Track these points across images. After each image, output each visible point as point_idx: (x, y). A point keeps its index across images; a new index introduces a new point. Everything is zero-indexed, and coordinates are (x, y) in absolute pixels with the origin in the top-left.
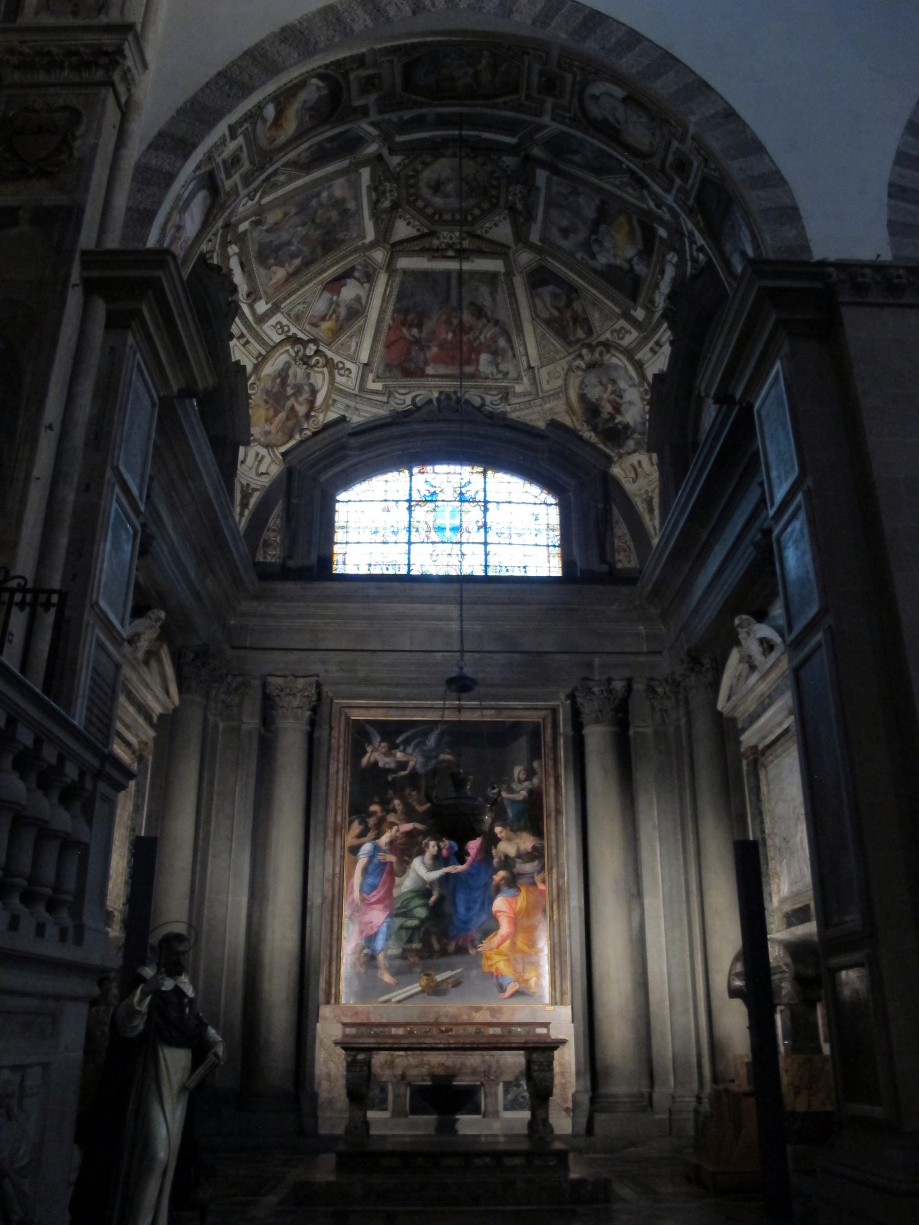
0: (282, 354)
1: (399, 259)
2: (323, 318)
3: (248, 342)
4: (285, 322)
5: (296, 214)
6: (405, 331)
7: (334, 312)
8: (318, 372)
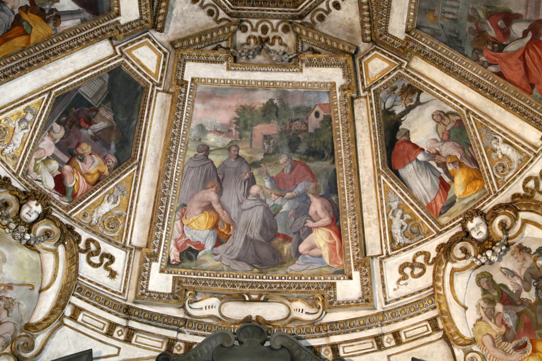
0: (452, 283)
1: (390, 32)
2: (445, 187)
4: (407, 256)
5: (220, 192)
6: (511, 48)
7: (443, 165)
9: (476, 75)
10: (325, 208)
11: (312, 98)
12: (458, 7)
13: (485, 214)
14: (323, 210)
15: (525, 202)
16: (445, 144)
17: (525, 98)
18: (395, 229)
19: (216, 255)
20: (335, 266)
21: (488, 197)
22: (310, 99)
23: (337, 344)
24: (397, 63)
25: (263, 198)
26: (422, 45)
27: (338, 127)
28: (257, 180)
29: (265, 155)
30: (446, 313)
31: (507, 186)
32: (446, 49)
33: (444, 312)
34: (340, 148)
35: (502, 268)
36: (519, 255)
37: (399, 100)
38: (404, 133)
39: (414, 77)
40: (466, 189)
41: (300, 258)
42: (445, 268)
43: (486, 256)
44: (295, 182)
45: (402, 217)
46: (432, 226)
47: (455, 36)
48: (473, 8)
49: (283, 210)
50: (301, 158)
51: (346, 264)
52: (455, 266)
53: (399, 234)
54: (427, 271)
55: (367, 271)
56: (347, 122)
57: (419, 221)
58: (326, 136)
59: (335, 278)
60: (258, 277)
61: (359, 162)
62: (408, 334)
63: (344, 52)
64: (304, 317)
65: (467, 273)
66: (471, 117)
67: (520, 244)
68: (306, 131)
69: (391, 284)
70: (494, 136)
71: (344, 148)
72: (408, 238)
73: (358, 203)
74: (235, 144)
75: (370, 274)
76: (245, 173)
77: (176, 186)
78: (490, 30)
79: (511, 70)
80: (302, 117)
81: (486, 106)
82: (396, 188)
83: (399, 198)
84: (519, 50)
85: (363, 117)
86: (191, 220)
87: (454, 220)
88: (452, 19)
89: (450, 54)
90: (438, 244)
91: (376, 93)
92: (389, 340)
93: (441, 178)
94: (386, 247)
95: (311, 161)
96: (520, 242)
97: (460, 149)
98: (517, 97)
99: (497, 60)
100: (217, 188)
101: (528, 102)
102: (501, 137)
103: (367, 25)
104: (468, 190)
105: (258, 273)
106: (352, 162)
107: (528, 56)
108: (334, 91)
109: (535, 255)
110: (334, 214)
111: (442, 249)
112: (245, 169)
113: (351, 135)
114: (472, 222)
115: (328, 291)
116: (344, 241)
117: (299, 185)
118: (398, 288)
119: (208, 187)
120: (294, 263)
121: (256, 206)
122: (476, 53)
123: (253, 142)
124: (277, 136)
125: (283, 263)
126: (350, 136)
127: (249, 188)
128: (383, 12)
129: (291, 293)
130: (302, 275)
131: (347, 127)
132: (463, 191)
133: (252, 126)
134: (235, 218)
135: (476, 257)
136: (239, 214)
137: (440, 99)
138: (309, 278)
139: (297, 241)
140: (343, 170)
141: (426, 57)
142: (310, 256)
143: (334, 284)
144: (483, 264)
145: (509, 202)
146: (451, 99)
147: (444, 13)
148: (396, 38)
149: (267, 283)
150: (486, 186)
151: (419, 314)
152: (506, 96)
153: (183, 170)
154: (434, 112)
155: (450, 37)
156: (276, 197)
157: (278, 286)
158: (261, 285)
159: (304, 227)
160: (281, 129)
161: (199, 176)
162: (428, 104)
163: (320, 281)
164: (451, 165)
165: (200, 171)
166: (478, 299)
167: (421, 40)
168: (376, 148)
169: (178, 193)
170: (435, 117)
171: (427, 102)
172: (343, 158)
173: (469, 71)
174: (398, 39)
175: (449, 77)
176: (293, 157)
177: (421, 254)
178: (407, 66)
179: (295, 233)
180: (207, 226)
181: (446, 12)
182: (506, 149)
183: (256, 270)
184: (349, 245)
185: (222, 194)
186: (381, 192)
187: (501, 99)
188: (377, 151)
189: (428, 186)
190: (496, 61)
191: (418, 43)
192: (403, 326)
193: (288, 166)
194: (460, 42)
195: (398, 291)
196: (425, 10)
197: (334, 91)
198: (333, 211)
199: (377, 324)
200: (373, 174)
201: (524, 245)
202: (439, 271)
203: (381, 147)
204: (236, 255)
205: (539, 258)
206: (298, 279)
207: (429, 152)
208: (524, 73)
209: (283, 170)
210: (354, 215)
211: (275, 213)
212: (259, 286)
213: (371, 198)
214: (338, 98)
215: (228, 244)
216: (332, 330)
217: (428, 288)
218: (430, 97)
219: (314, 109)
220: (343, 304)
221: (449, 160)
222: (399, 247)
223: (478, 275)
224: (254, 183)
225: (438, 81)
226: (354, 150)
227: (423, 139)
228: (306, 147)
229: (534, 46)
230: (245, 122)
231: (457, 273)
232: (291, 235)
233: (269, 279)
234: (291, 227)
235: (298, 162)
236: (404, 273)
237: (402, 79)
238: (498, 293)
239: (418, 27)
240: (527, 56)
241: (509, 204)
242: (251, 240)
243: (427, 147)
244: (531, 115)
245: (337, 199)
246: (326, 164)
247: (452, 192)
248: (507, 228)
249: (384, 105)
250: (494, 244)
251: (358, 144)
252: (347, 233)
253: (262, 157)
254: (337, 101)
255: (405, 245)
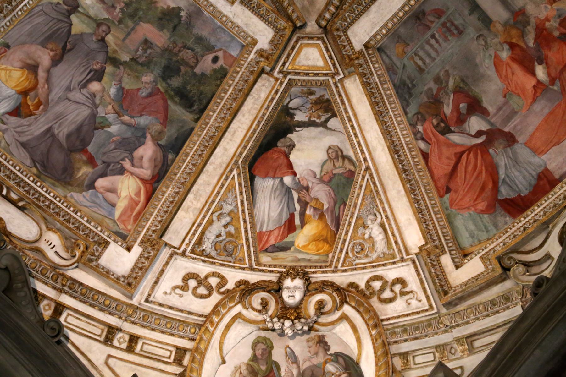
0: (228, 327)
1: (349, 33)
3: (133, 339)
4: (203, 269)
5: (56, 61)
6: (455, 138)
7: (304, 205)
8: (333, 323)
9: (402, 139)
10: (154, 160)
11: (223, 40)
12: (434, 59)
13: (310, 283)
14: (150, 160)
15: (358, 298)
16: (321, 185)
17: (432, 197)
18: (210, 232)
19: (3, 123)
20: (122, 226)
21: (326, 267)
22: (220, 39)
23: (65, 307)
24: (332, 69)
25: (98, 102)
26: (371, 71)
27: (228, 88)
28: (105, 78)
29: (132, 59)
30: (202, 353)
31: (353, 270)
32: (392, 92)
33: (200, 351)
34: (214, 111)
35: (288, 347)
36: (314, 346)
37: (307, 107)
38: (288, 144)
39: (340, 95)
40: (309, 244)
41: (90, 191)
42: (232, 307)
43: (283, 324)
44: (143, 110)
45: (225, 226)
46: (249, 256)
47: (410, 85)
48: (447, 71)
49: (108, 129)
50: (166, 91)
51: (134, 232)
52: (245, 312)
53: (211, 241)
54: (211, 297)
55: (152, 254)
56: (241, 90)
57: (240, 242)
58: (208, 88)
59: (112, 238)
60: (31, 179)
61: (223, 140)
62: (146, 347)
63: (289, 18)
64: (51, 254)
65: (251, 328)
66: (367, 176)
67: (323, 336)
68: (192, 68)
69: (166, 284)
70: (376, 212)
71: (218, 114)
72: (217, 251)
73: (193, 179)
74: (109, 24)
75: (152, 260)
76: (98, 63)
77: (14, 19)
78: (448, 105)
79: (440, 159)
80: (199, 50)
81: (388, 177)
82: (241, 193)
83: (237, 205)
84: (462, 145)
85: (259, 97)
86: (4, 66)
87: (275, 266)
88: (419, 67)
89: (392, 99)
90: (243, 278)
91: (291, 83)
92: (122, 340)
93: (292, 216)
94: (188, 244)
95: (175, 103)
96: (324, 334)
97: (332, 201)
98: (426, 190)
99: (433, 139)
100: (56, 55)
101: (433, 202)
102: (382, 218)
103: (332, 9)
104: (310, 247)
105: (35, 175)
106: (216, 134)
107: (466, 159)
108: (251, 49)
109: (330, 357)
110: (158, 173)
111: (243, 287)
112: (101, 57)
113: (236, 106)
114: (293, 279)
115: (96, 246)
116: (150, 208)
117: (145, 117)
118: (170, 294)
119: (48, 46)
120: (81, 192)
121: (84, 104)
122: (418, 117)
123: (129, 37)
124: (159, 50)
125: (69, 184)
126: (233, 106)
127: (90, 81)
128: (357, 8)
129: (55, 220)
130: (80, 211)
131: (237, 95)
132: (305, 244)
133: (140, 19)
134: (52, 101)
135: (271, 317)
136: (60, 100)
137: (349, 137)
138: (86, 219)
139: (100, 172)
140: (201, 135)
141: (366, 85)
142: (103, 197)
143: (107, 244)
144: (273, 330)
145: (342, 286)
146: (360, 145)
147: (416, 54)
148: (351, 43)
149: (37, 191)
150: (331, 255)
151: (172, 335)
152: (416, 181)
153: (33, 8)
154: (333, 146)
155: (404, 84)
156: (112, 111)
157: (47, 203)
158: (30, 189)
159: (118, 163)
160: (168, 46)
161: (46, 28)
162: (333, 132)
163: (95, 230)
164: (312, 210)
165: (51, 24)
166: (242, 361)
167: (373, 64)
168: (250, 138)
169: (10, 29)
170: (330, 151)
171: (334, 130)
172: (210, 123)
173: (398, 131)
174: (352, 46)
175: (375, 121)
176: (159, 83)
177: (218, 277)
178: (341, 80)
179: (104, 162)
180: (16, 86)
181: (419, 56)
182: (377, 233)
183: (34, 170)
184: (151, 215)
185: (56, 65)
186: (223, 185)
187: (409, 181)
188: (248, 141)
189: (274, 214)
190: (431, 139)
191: (369, 65)
192: (147, 336)
193: (147, 89)
194: (411, 95)
195: (168, 297)
196: (399, 37)
197: (251, 49)
198: (160, 169)
199: (122, 315)
200: (227, 162)
201: (327, 339)
202: (224, 306)
203: (256, 140)
204: (24, 139)
205: (332, 363)
206: (73, 211)
207: (300, 182)
208: (450, 170)
209: (139, 89)
210: (180, 188)
211: (99, 126)
212: (27, 189)
213: (209, 184)
214: (249, 60)
215: (25, 121)
216: (71, 289)
217: (201, 316)
218: (340, 127)
219: (216, 52)
220: (102, 271)
221: (313, 204)
222: (200, 254)
223: (259, 337)
224: (99, 79)
225: (361, 117)
226: (227, 124)
227: (303, 163)
228: (180, 84)
229: (479, 152)
230: (137, 10)
231: (240, 320)
232: (99, 162)
233: (42, 189)
234: (104, 154)
235: (161, 93)
236: (187, 284)
237: (326, 89)
238: (267, 369)
239: (380, 50)
240: (465, 156)
241: (341, 288)
242: (53, 135)
243: (301, 175)
244: (427, 217)
245: (173, 160)
246: (188, 117)
247: (293, 237)
248: (322, 311)
249: (289, 102)
250: (298, 317)
251: (235, 121)
252: (159, 201)
253: (128, 60)
254: (245, 62)
255: (208, 256)
